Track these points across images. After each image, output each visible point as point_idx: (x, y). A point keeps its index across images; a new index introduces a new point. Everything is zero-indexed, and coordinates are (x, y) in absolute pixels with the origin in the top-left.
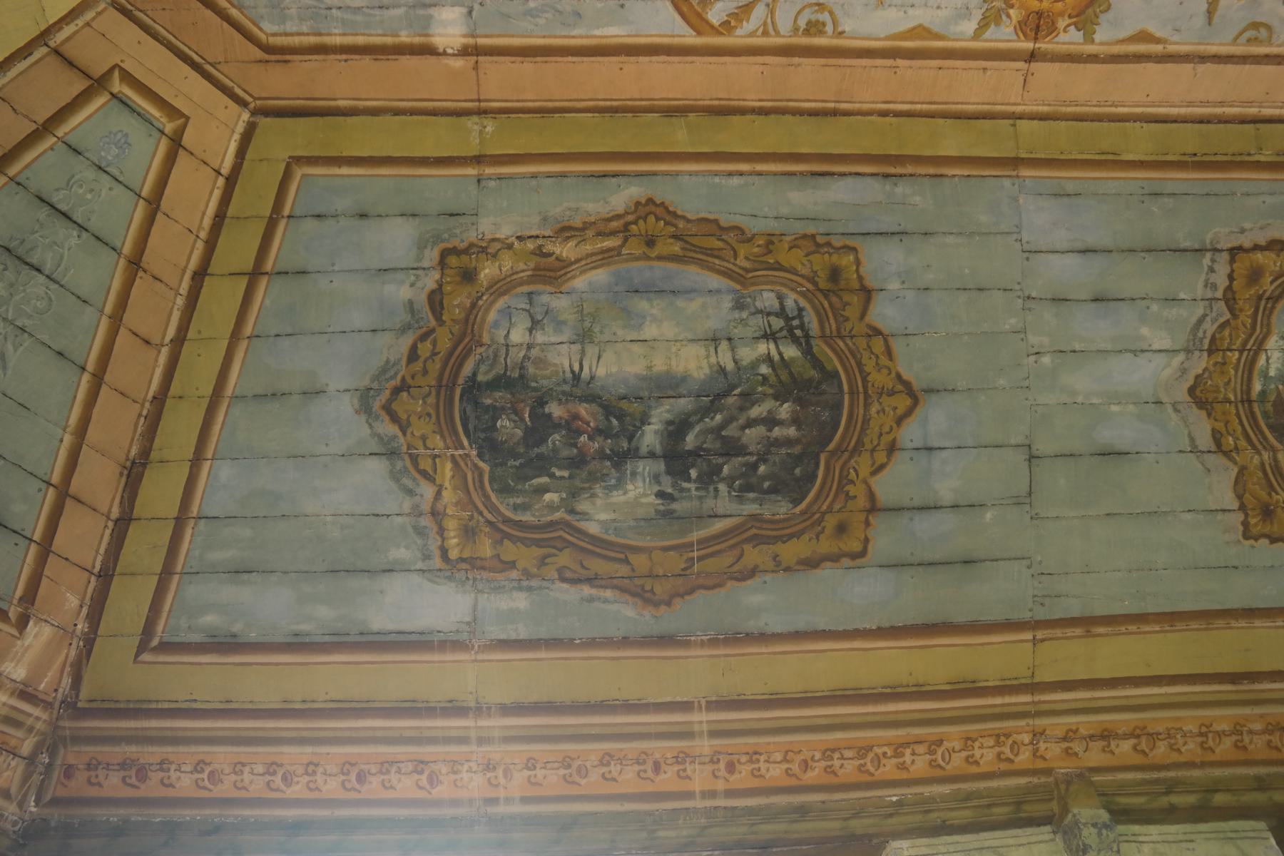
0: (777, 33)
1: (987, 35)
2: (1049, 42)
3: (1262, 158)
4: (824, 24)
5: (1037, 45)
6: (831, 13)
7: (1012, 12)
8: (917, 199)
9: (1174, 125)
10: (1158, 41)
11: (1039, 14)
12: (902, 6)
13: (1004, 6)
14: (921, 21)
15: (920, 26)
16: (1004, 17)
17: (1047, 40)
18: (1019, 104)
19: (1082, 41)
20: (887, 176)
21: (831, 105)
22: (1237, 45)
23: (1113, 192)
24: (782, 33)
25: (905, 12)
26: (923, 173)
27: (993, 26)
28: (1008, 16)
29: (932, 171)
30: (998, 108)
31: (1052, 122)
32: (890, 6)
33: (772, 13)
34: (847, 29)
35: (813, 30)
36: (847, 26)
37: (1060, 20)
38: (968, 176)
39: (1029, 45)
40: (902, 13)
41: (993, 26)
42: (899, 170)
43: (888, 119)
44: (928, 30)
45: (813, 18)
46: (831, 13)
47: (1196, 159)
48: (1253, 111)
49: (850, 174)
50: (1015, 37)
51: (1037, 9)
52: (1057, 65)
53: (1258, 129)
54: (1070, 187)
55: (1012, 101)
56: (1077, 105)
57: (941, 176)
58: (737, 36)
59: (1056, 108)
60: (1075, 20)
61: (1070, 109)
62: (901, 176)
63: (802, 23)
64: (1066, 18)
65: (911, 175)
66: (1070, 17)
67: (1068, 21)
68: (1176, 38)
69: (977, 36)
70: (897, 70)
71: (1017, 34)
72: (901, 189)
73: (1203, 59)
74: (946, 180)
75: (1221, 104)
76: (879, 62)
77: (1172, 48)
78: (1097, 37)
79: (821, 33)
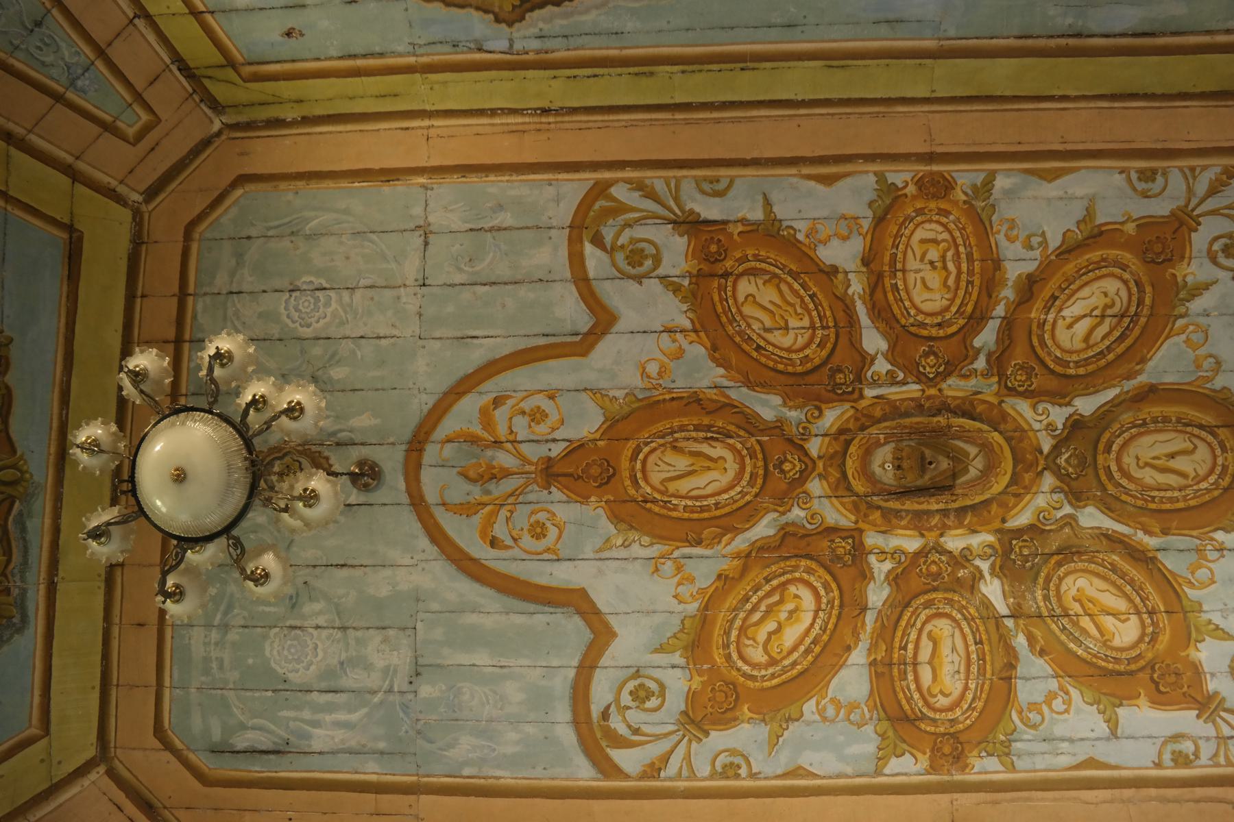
0: (1181, 169)
1: (982, 176)
2: (918, 172)
3: (668, 68)
4: (1140, 179)
5: (928, 168)
6: (1135, 189)
7: (964, 198)
8: (1051, 13)
9: (761, 98)
10: (809, 177)
11: (935, 197)
12: (1070, 198)
13: (973, 202)
14: (1050, 185)
15: (1050, 181)
16: (970, 192)
17: (921, 174)
18: (929, 112)
19: (887, 174)
20: (1078, 35)
21: (1116, 105)
22: (727, 176)
23: (836, 27)
24: (1177, 170)
25: (1066, 192)
26: (1040, 39)
27: (979, 184)
28: (966, 194)
29: (1030, 42)
30: (949, 108)
31: (893, 96)
32: (1082, 198)
33: (1190, 190)
34: (1117, 176)
35: (1149, 174)
36: (1118, 179)
37: (914, 192)
38: (992, 38)
39: (935, 168)
40: (1070, 191)
41: (979, 184)
42: (1063, 41)
43: (1060, 93)
44: (1041, 177)
45: (1150, 185)
46: (1135, 189)
47: (742, 65)
48: (679, 116)
49: (1115, 36)
50: (954, 174)
51: (939, 201)
52: (902, 150)
53: (672, 98)
54: (884, 30)
55: (937, 116)
56: (869, 113)
57: (1020, 37)
58: (1219, 165)
59: (890, 110)
60: (900, 193)
61: (876, 109)
62: (1063, 36)
63: (1160, 180)
64: (909, 195)
65: (1052, 37)
66: (906, 195)
67: (907, 191)
68: (795, 180)
69: (991, 176)
70: (1061, 140)
71: (952, 177)
72: (1067, 21)
73: (756, 162)
74: (1016, 33)
75: (718, 121)
76: (1080, 147)
77: (793, 171)
78: (873, 179)
79: (1141, 172)
